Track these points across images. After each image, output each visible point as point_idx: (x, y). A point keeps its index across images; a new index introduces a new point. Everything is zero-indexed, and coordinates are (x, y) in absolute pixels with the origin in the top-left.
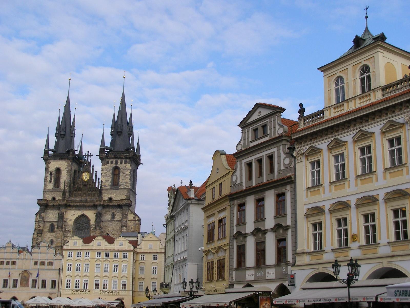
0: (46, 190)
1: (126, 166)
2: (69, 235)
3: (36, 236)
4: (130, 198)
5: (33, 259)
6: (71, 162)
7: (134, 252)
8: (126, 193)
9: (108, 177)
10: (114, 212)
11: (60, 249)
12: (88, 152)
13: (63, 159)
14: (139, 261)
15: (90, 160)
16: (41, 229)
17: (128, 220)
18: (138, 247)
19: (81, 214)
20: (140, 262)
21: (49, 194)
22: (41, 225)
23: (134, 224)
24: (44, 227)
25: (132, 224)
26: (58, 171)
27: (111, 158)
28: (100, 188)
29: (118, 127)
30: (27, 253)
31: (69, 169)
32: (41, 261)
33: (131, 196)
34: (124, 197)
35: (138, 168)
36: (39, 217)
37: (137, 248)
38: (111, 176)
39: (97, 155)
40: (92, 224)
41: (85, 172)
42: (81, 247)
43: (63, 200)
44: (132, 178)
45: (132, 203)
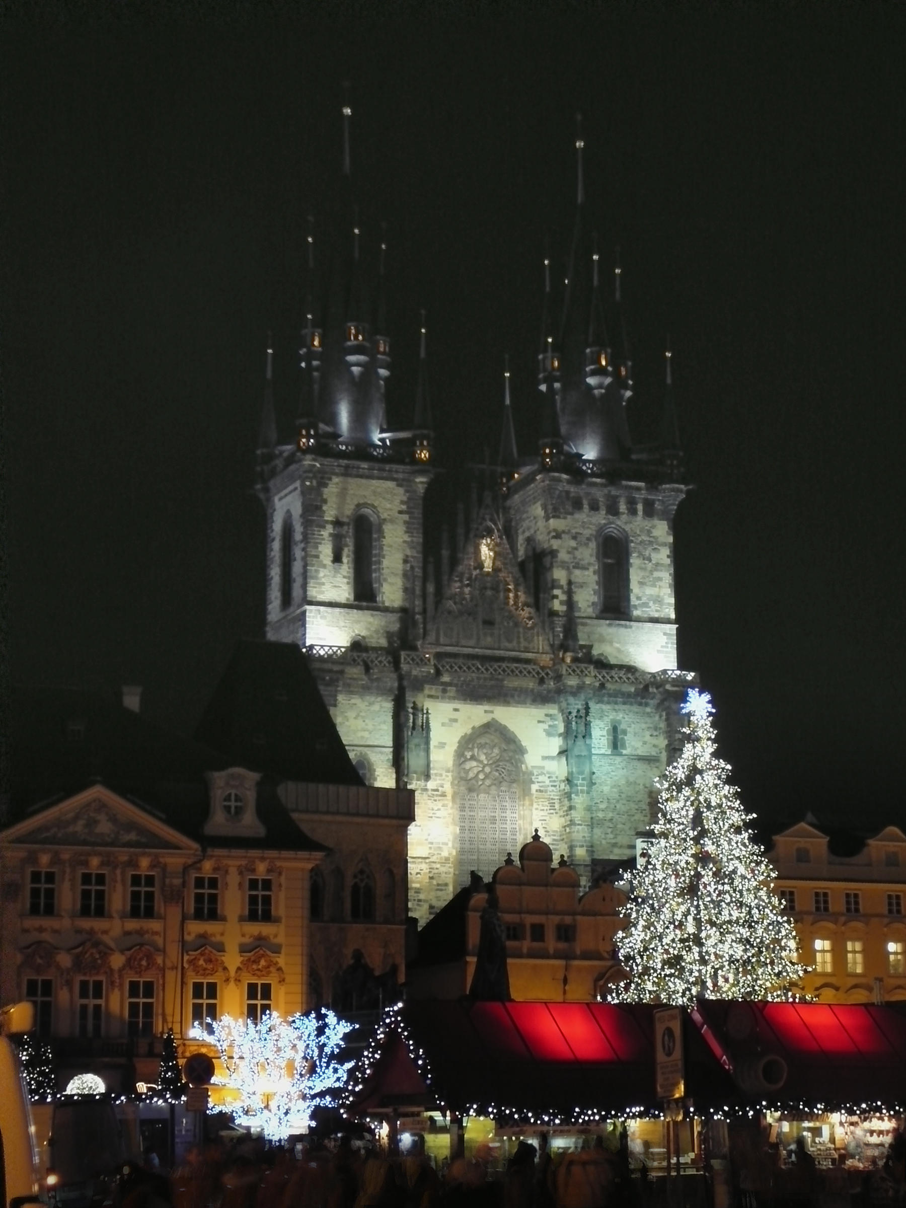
2: (439, 810)
19: (485, 721)
40: (532, 767)
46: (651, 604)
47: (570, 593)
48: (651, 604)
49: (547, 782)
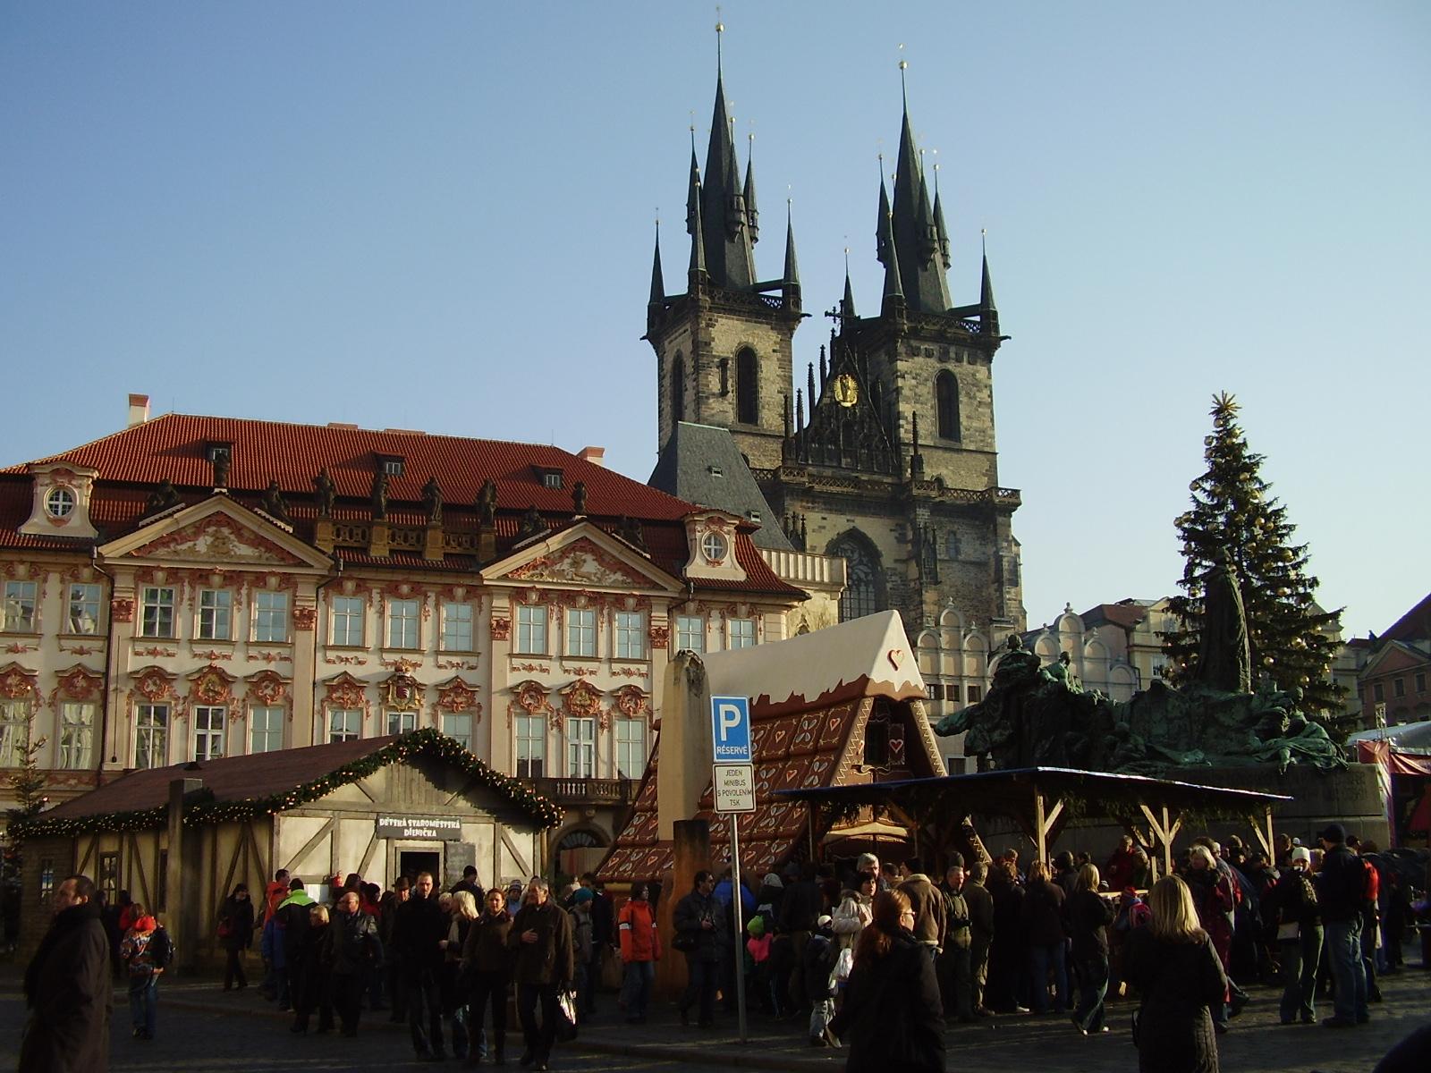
8: (986, 468)
10: (954, 529)
19: (848, 528)
27: (925, 339)
29: (929, 236)
31: (785, 356)
47: (914, 422)
49: (899, 582)
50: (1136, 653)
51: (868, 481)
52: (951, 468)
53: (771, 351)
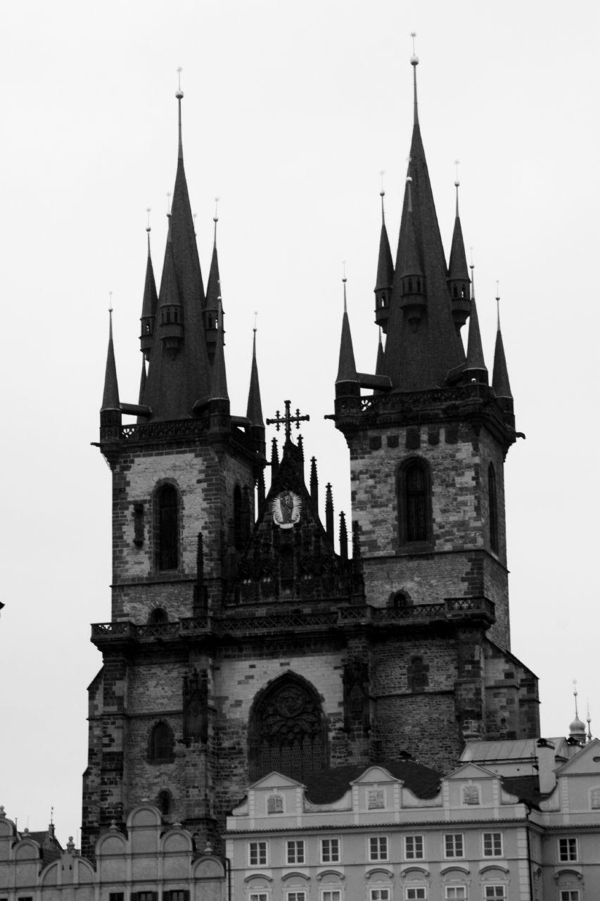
0: (123, 580)
1: (457, 454)
2: (236, 767)
3: (98, 780)
4: (485, 592)
5: (102, 884)
6: (216, 452)
7: (532, 826)
8: (465, 571)
9: (381, 505)
10: (419, 654)
11: (202, 831)
12: (288, 403)
13: (182, 443)
14: (553, 866)
15: (300, 438)
16: (115, 748)
17: (483, 690)
18: (542, 805)
19: (281, 673)
20: (557, 870)
21: (138, 595)
22: (117, 734)
23: (510, 701)
24: (128, 740)
25: (505, 704)
26: (167, 494)
28: (350, 556)
29: (407, 289)
30: (77, 860)
31: (213, 484)
32: (138, 888)
33: (487, 579)
34: (459, 589)
35: (507, 455)
36: (105, 698)
37: (538, 809)
38: (396, 502)
39: (327, 414)
41: (282, 490)
42: (299, 819)
43: (199, 620)
44: (487, 504)
45: (493, 613)
46: (455, 530)
48: (455, 530)
50: (227, 842)
51: (312, 615)
52: (419, 579)
53: (194, 481)
